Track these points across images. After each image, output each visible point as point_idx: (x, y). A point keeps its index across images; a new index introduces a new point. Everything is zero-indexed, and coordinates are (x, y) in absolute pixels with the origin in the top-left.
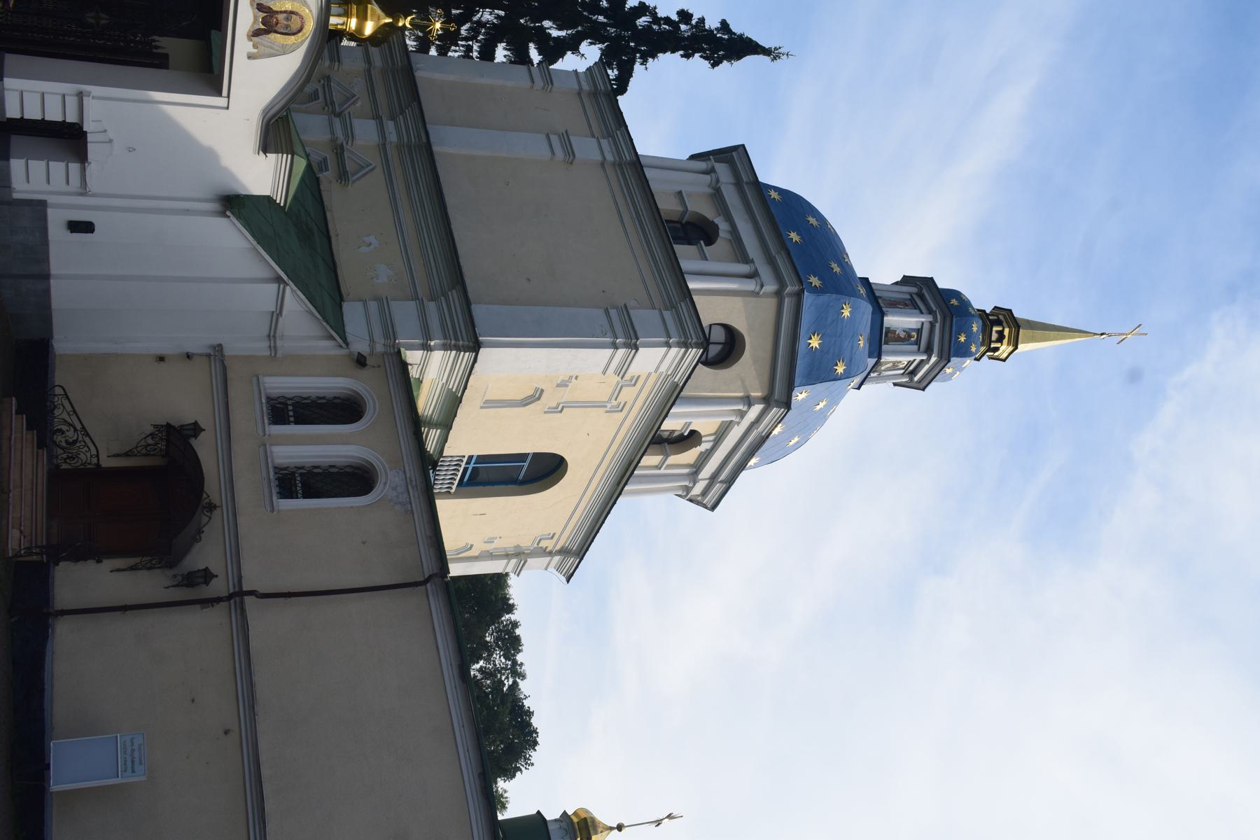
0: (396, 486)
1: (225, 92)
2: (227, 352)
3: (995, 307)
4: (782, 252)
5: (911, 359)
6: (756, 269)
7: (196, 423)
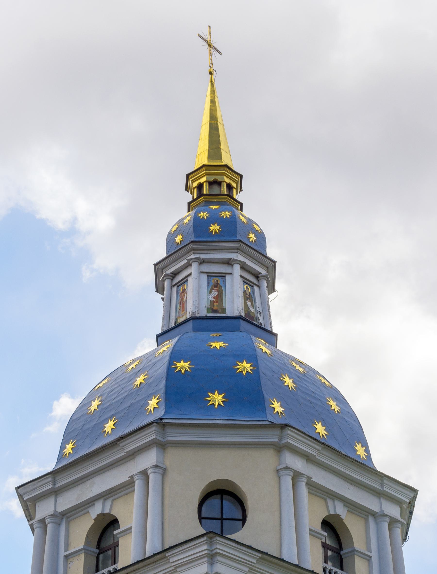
3: (186, 189)
5: (240, 281)
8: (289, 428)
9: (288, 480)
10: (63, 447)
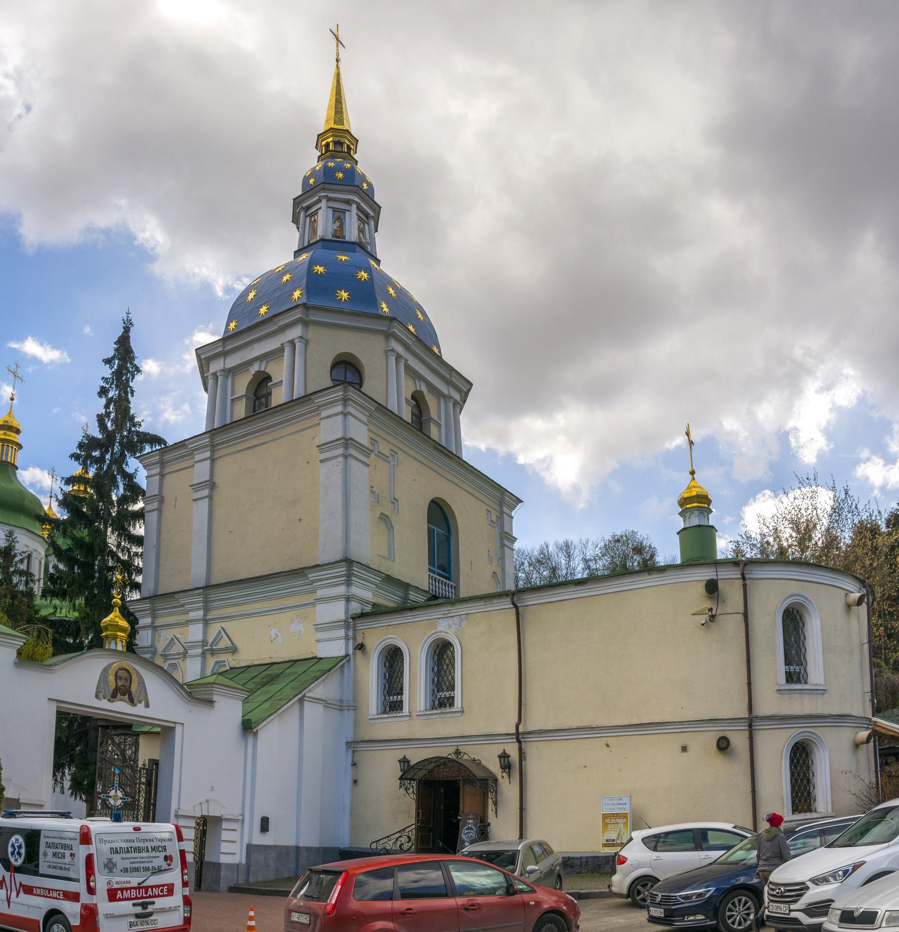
0: (449, 625)
2: (350, 740)
3: (316, 148)
4: (275, 321)
5: (356, 218)
6: (289, 342)
9: (393, 359)
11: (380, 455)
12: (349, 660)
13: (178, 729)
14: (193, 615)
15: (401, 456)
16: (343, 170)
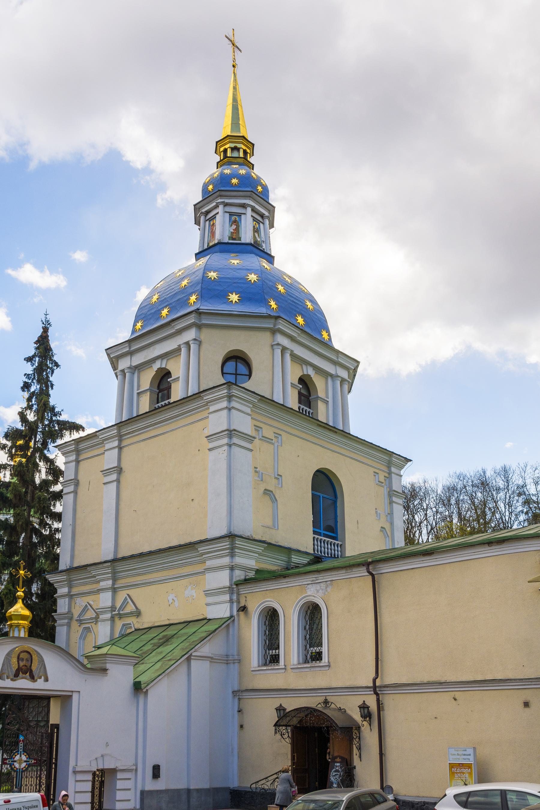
0: (316, 590)
1: (70, 694)
2: (236, 689)
3: (216, 153)
5: (251, 219)
7: (277, 709)
8: (281, 319)
9: (278, 352)
10: (135, 325)
11: (265, 439)
12: (234, 620)
13: (75, 697)
14: (103, 584)
15: (284, 436)
16: (238, 176)
